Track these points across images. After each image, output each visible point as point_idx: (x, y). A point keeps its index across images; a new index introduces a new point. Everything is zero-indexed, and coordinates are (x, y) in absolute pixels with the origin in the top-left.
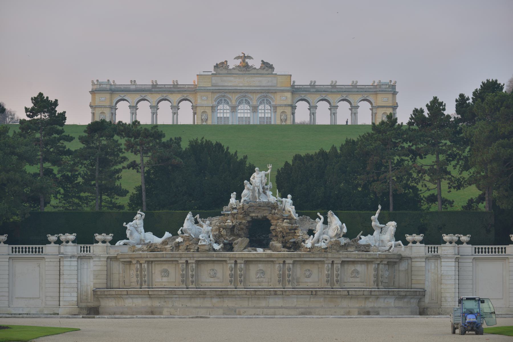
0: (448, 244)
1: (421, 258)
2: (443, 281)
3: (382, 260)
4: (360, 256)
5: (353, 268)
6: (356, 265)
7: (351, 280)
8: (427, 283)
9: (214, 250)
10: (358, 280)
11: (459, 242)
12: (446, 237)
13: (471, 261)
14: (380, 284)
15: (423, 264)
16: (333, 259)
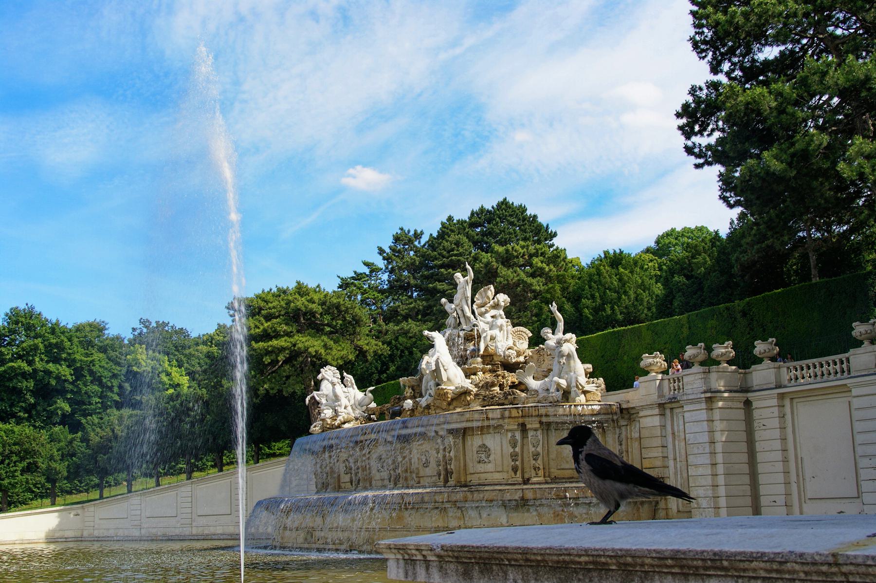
0: (696, 368)
1: (650, 406)
2: (691, 459)
3: (521, 420)
4: (464, 418)
5: (480, 443)
6: (484, 436)
7: (481, 468)
8: (671, 463)
9: (339, 427)
10: (490, 467)
11: (745, 359)
12: (690, 352)
13: (775, 402)
14: (533, 473)
15: (656, 421)
16: (434, 428)
